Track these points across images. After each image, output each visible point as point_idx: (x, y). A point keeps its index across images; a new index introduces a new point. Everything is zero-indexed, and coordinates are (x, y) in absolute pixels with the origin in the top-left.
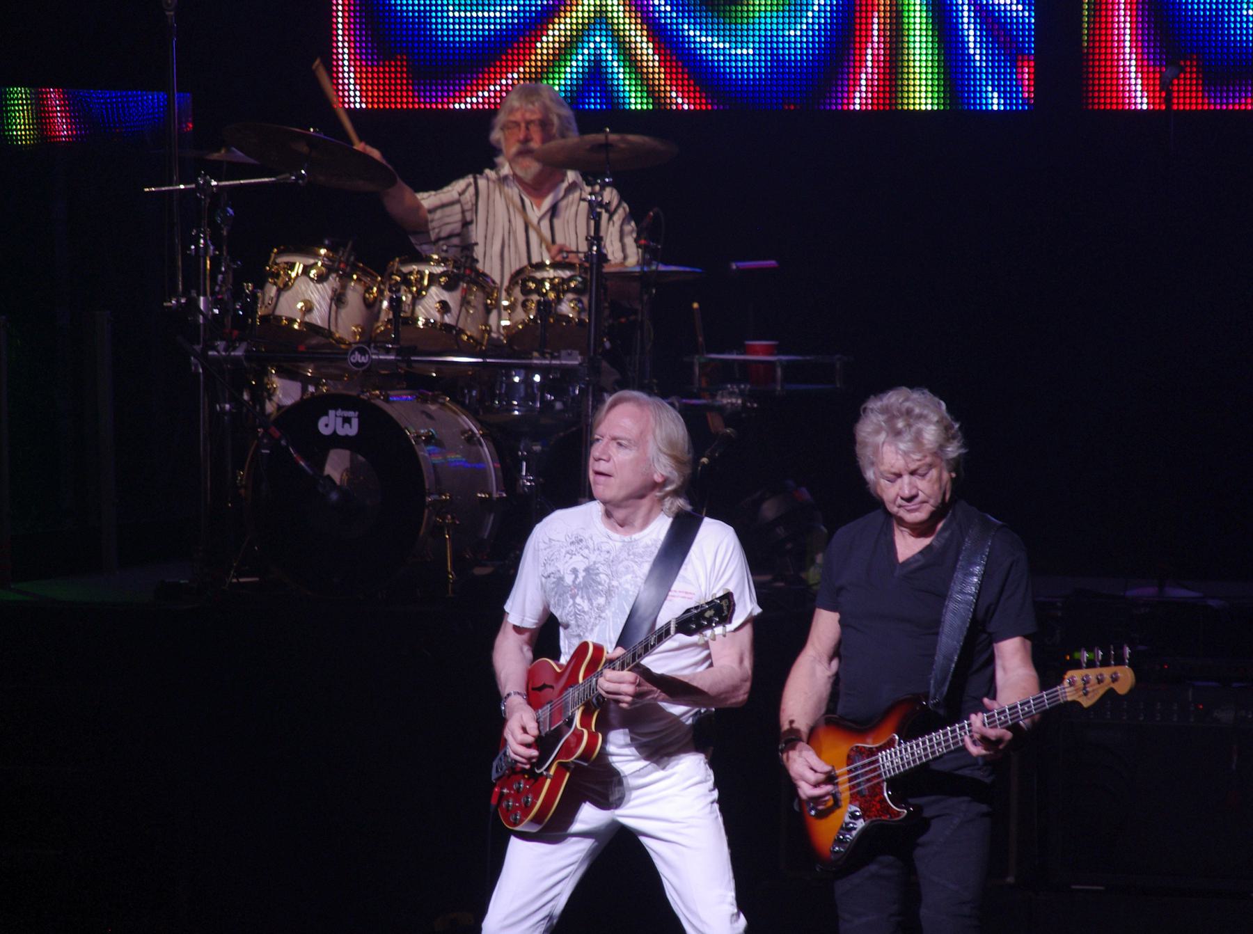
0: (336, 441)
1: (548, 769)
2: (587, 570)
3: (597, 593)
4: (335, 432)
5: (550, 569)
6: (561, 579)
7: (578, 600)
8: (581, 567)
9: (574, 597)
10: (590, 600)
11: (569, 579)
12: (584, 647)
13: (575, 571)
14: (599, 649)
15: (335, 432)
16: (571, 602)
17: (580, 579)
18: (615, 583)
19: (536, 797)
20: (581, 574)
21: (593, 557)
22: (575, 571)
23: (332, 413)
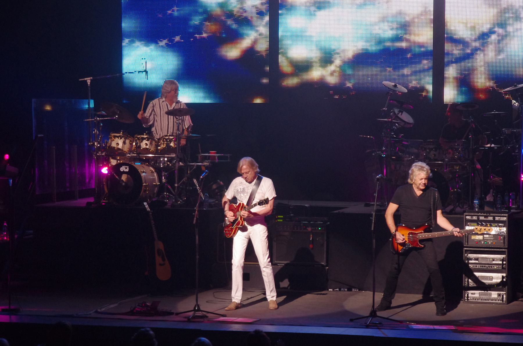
0: (124, 172)
1: (234, 227)
2: (243, 189)
3: (245, 193)
4: (124, 171)
5: (236, 188)
6: (238, 190)
7: (241, 194)
8: (242, 188)
9: (240, 194)
10: (244, 194)
11: (239, 190)
12: (240, 204)
13: (241, 189)
14: (243, 204)
15: (124, 171)
16: (240, 195)
17: (242, 190)
18: (248, 191)
19: (232, 232)
20: (242, 189)
21: (244, 186)
22: (241, 189)
23: (123, 167)
